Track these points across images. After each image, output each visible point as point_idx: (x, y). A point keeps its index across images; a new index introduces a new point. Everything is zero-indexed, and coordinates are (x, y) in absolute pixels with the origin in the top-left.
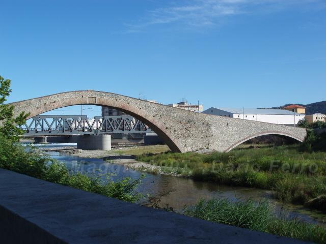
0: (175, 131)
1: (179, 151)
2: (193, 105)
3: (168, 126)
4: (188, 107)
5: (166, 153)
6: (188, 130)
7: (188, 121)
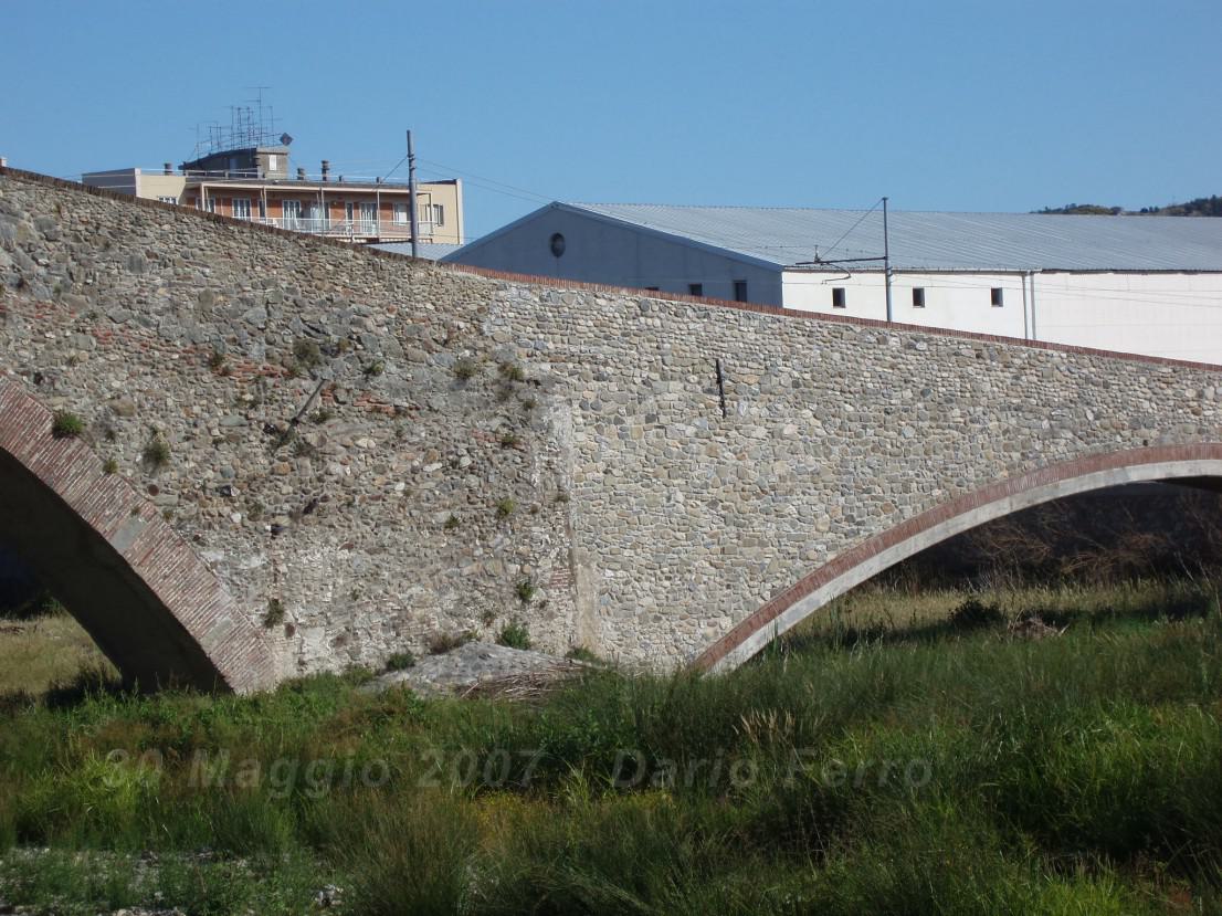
0: (156, 456)
1: (204, 675)
2: (355, 173)
3: (81, 406)
4: (303, 201)
5: (63, 698)
6: (303, 450)
7: (303, 352)
